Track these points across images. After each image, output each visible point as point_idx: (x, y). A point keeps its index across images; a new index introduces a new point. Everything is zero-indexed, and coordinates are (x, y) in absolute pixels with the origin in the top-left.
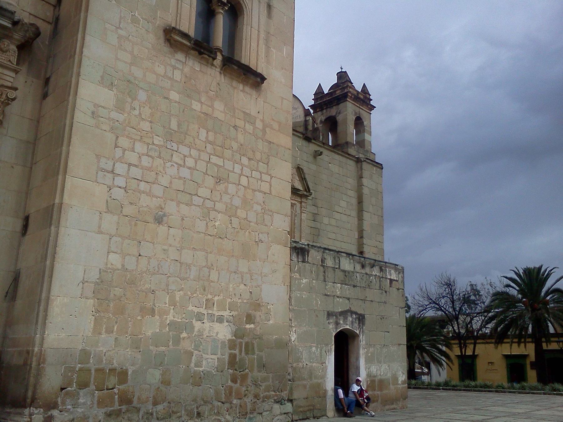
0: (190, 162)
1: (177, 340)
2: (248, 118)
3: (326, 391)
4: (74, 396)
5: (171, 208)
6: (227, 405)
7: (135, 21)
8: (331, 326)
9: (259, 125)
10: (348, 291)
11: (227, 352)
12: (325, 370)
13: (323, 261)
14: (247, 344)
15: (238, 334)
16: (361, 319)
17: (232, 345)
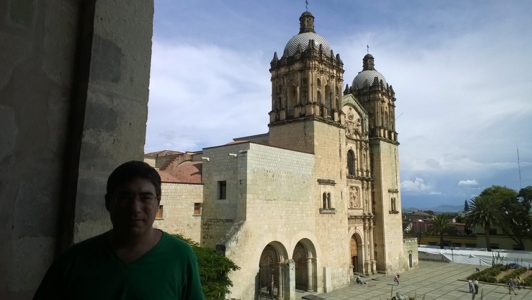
10: (410, 246)
15: (399, 258)
16: (412, 251)
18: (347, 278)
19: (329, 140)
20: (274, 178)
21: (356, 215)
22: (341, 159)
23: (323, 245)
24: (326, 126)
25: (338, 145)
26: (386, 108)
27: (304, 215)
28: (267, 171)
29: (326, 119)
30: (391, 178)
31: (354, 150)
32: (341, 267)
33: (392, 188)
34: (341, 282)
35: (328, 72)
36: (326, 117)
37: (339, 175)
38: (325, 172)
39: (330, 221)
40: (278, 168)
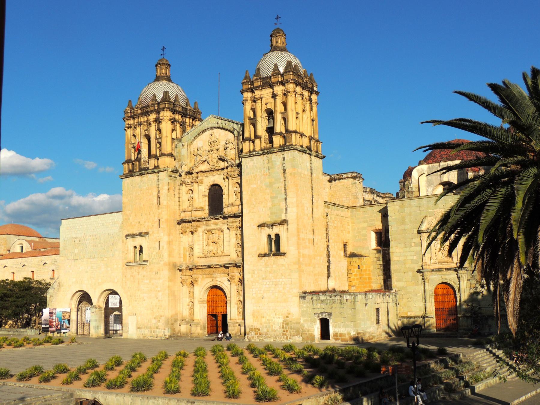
0: (268, 283)
1: (269, 323)
2: (283, 265)
3: (314, 336)
4: (251, 333)
5: (265, 295)
6: (283, 337)
7: (253, 257)
8: (316, 317)
9: (286, 266)
10: (323, 306)
11: (282, 325)
12: (314, 330)
13: (312, 298)
14: (287, 323)
15: (285, 321)
16: (330, 314)
17: (283, 323)
18: (163, 330)
19: (142, 192)
20: (81, 242)
21: (207, 264)
22: (160, 206)
23: (131, 296)
24: (137, 179)
25: (155, 193)
26: (266, 104)
27: (109, 269)
28: (75, 238)
29: (137, 172)
30: (271, 206)
31: (219, 183)
32: (155, 318)
33: (270, 220)
34: (154, 332)
35: (144, 122)
36: (137, 170)
37: (157, 224)
38: (135, 225)
39: (140, 274)
40: (84, 234)
